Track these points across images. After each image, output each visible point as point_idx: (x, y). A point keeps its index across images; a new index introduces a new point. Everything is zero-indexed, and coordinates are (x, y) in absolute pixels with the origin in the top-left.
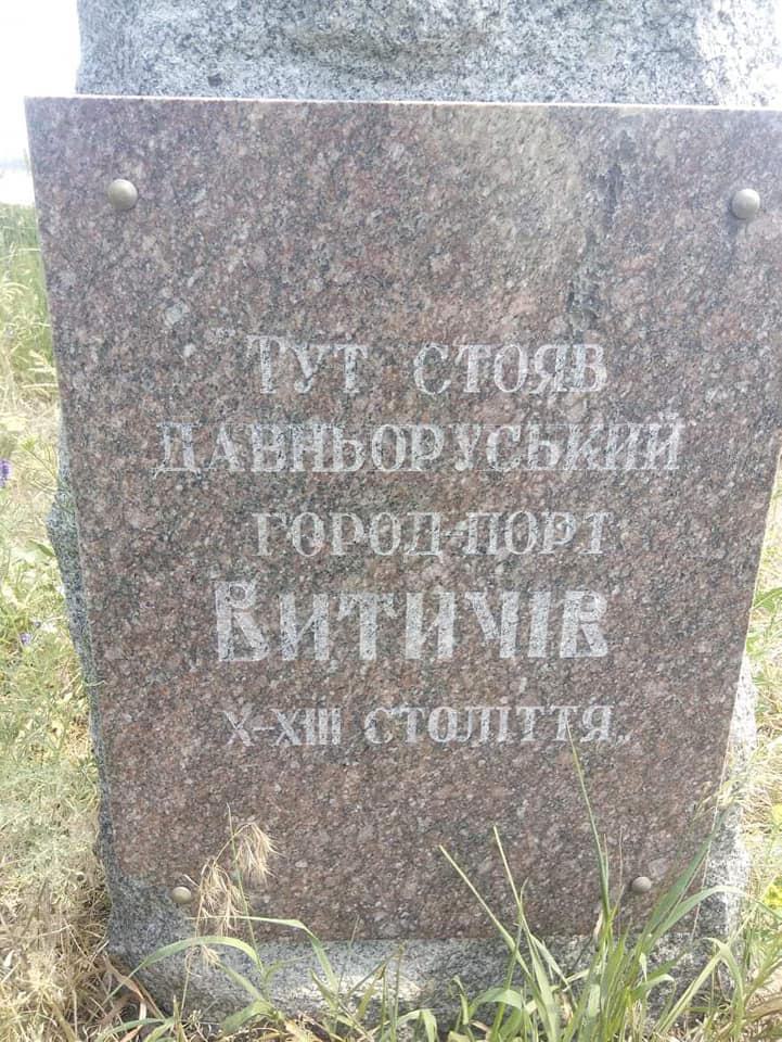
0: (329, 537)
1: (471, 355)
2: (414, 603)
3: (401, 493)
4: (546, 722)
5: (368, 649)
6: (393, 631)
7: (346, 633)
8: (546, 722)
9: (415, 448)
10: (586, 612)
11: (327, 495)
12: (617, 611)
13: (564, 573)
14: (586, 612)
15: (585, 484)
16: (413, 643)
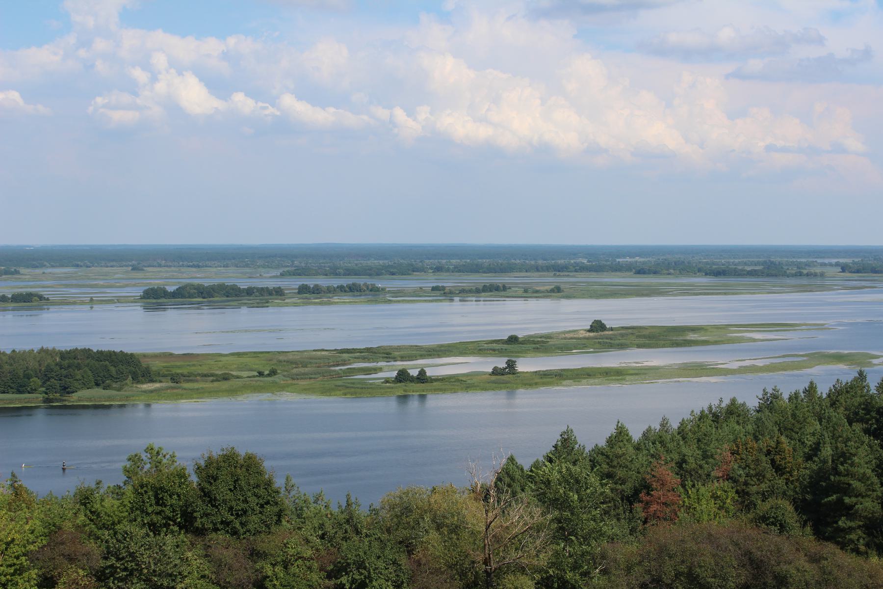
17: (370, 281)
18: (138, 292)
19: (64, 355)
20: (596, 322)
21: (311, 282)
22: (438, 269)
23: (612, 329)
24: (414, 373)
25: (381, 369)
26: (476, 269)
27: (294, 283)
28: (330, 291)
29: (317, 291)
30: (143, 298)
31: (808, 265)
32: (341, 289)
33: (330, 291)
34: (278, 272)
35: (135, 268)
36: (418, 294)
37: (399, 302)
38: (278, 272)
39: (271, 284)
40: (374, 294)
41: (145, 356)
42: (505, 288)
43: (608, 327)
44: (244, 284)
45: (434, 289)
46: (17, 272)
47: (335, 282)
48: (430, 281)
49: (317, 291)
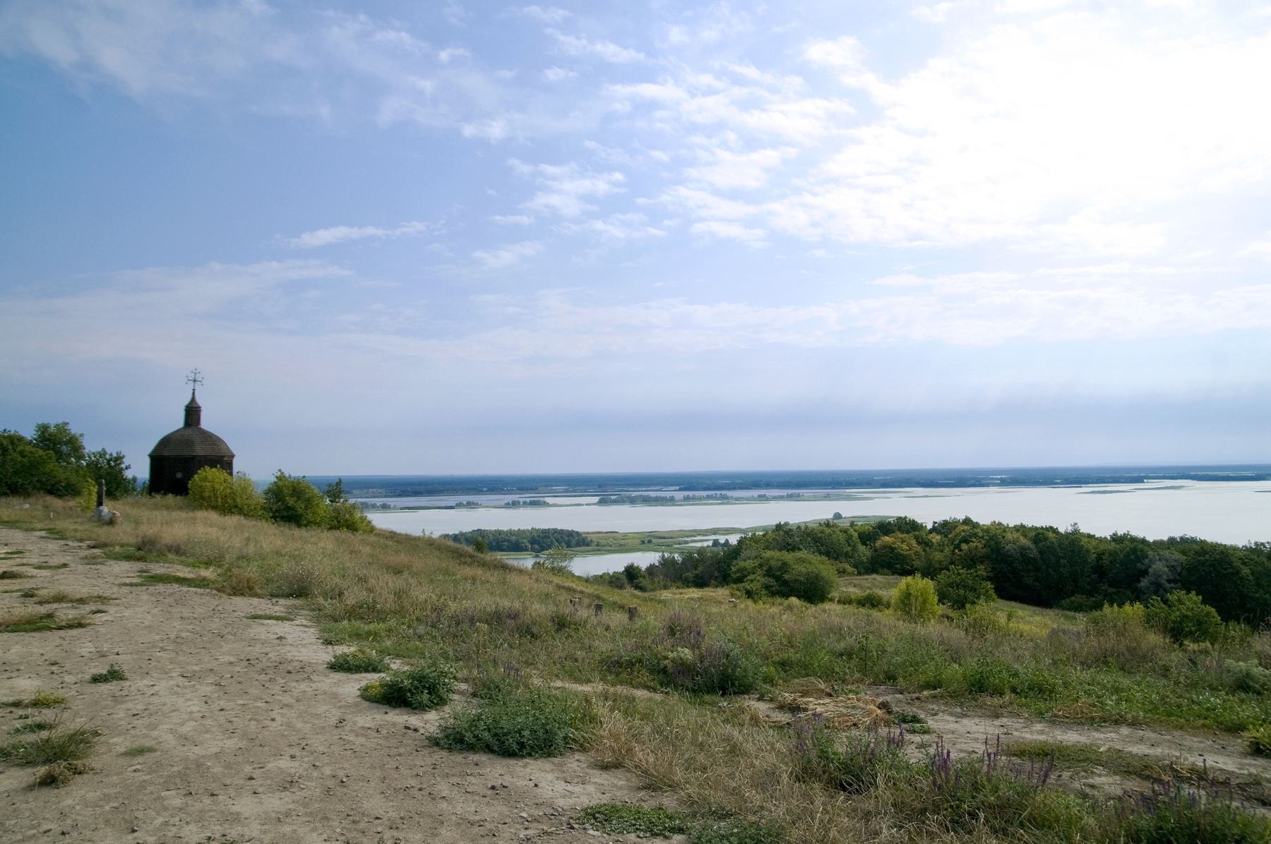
18: (596, 499)
19: (544, 531)
23: (845, 518)
24: (722, 541)
25: (706, 540)
28: (700, 498)
29: (694, 498)
30: (598, 502)
31: (983, 479)
33: (700, 498)
34: (678, 488)
36: (752, 499)
37: (738, 504)
38: (678, 488)
39: (668, 494)
41: (588, 533)
42: (799, 495)
43: (843, 516)
44: (653, 494)
45: (759, 496)
46: (536, 489)
48: (755, 493)
49: (694, 498)
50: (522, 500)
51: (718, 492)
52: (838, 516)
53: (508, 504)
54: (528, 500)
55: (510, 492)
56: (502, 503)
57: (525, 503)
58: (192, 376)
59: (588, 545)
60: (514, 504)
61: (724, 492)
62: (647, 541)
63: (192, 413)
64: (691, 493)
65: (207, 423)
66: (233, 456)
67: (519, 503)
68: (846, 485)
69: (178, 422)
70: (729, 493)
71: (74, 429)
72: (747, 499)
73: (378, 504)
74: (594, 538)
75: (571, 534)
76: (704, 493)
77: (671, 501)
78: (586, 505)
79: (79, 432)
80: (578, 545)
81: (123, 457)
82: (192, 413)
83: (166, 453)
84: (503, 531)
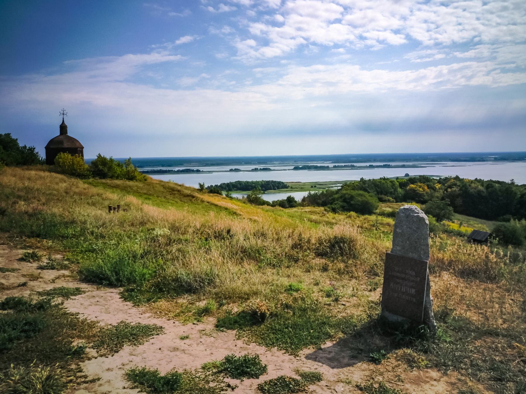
0: (398, 281)
1: (407, 271)
2: (403, 287)
3: (403, 279)
4: (411, 299)
5: (399, 289)
6: (401, 288)
7: (398, 288)
8: (411, 299)
9: (403, 276)
10: (413, 291)
11: (398, 278)
12: (416, 291)
13: (412, 287)
14: (413, 291)
15: (413, 281)
16: (402, 289)
17: (352, 164)
18: (293, 167)
20: (406, 174)
21: (337, 165)
22: (375, 161)
26: (381, 161)
27: (331, 165)
29: (338, 167)
32: (345, 166)
33: (342, 167)
35: (295, 161)
39: (326, 165)
40: (353, 167)
41: (287, 183)
42: (389, 165)
44: (319, 165)
45: (370, 165)
46: (266, 163)
47: (343, 164)
48: (368, 164)
50: (259, 168)
51: (350, 164)
52: (407, 175)
53: (253, 169)
54: (262, 168)
55: (255, 164)
56: (251, 169)
57: (260, 169)
58: (62, 112)
59: (287, 188)
60: (256, 170)
61: (352, 164)
62: (314, 186)
63: (63, 128)
64: (337, 165)
65: (70, 133)
66: (83, 148)
67: (258, 169)
68: (413, 160)
69: (58, 133)
70: (355, 164)
71: (14, 137)
72: (364, 167)
73: (195, 170)
74: (290, 185)
75: (280, 183)
76: (343, 164)
77: (327, 168)
78: (288, 170)
79: (15, 138)
80: (283, 188)
81: (35, 148)
82: (63, 128)
83: (51, 147)
84: (249, 182)
